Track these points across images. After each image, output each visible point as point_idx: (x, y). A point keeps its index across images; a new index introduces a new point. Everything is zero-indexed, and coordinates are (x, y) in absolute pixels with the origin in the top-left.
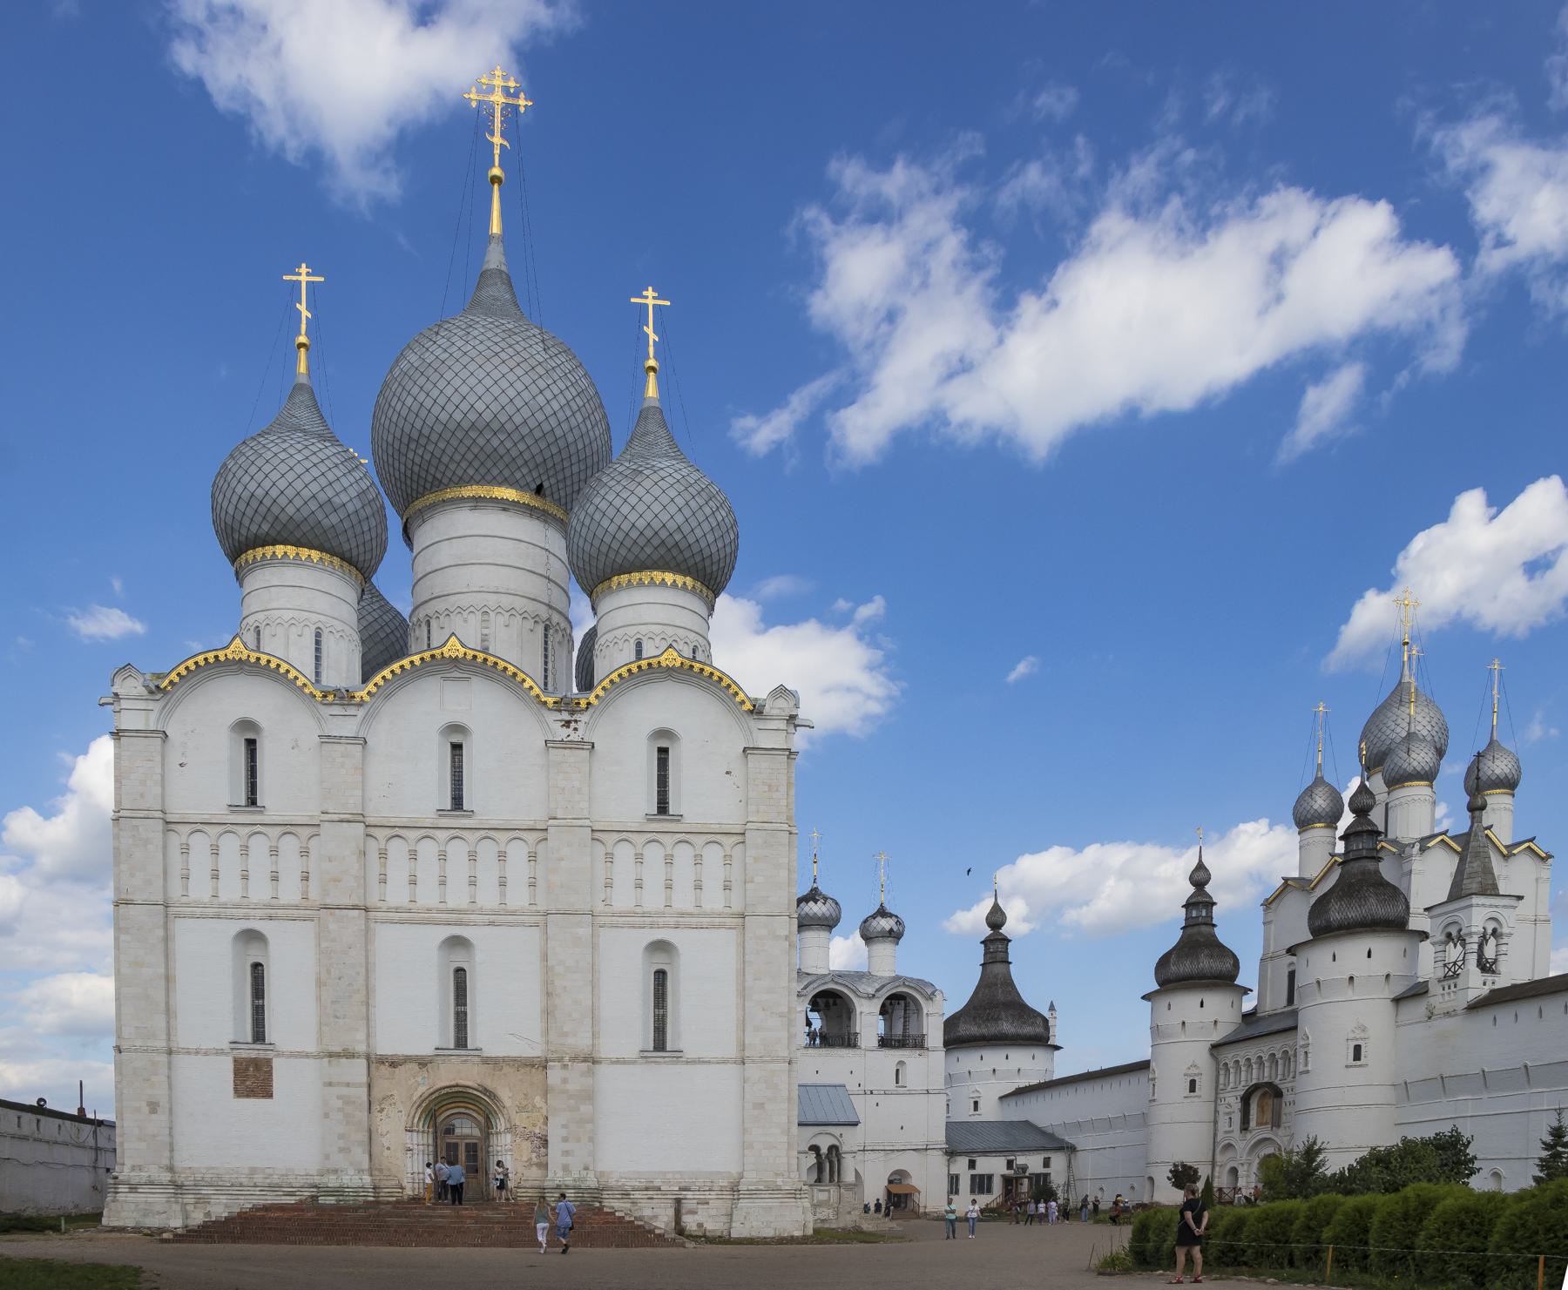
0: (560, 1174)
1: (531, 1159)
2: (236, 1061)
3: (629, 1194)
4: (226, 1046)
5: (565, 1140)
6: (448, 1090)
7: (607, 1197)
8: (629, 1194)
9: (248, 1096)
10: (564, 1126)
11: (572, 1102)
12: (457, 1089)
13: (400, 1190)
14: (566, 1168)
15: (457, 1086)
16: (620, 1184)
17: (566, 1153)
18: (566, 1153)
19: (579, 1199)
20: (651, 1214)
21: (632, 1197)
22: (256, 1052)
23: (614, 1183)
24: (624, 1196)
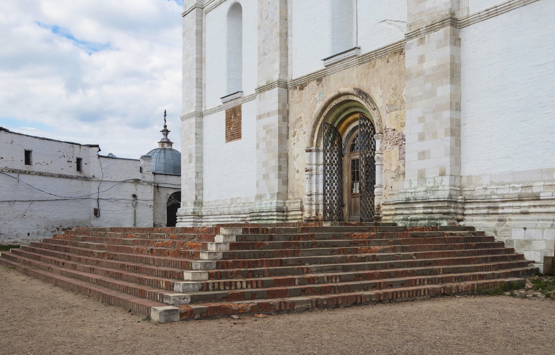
0: (415, 184)
1: (399, 167)
2: (227, 113)
3: (497, 208)
4: (220, 102)
5: (422, 138)
6: (336, 102)
7: (470, 212)
8: (497, 208)
9: (231, 140)
10: (421, 120)
11: (429, 85)
12: (343, 99)
13: (300, 213)
14: (422, 176)
15: (339, 95)
16: (488, 192)
17: (423, 155)
18: (423, 155)
19: (427, 216)
20: (522, 238)
21: (500, 211)
22: (233, 102)
23: (482, 192)
24: (491, 211)
